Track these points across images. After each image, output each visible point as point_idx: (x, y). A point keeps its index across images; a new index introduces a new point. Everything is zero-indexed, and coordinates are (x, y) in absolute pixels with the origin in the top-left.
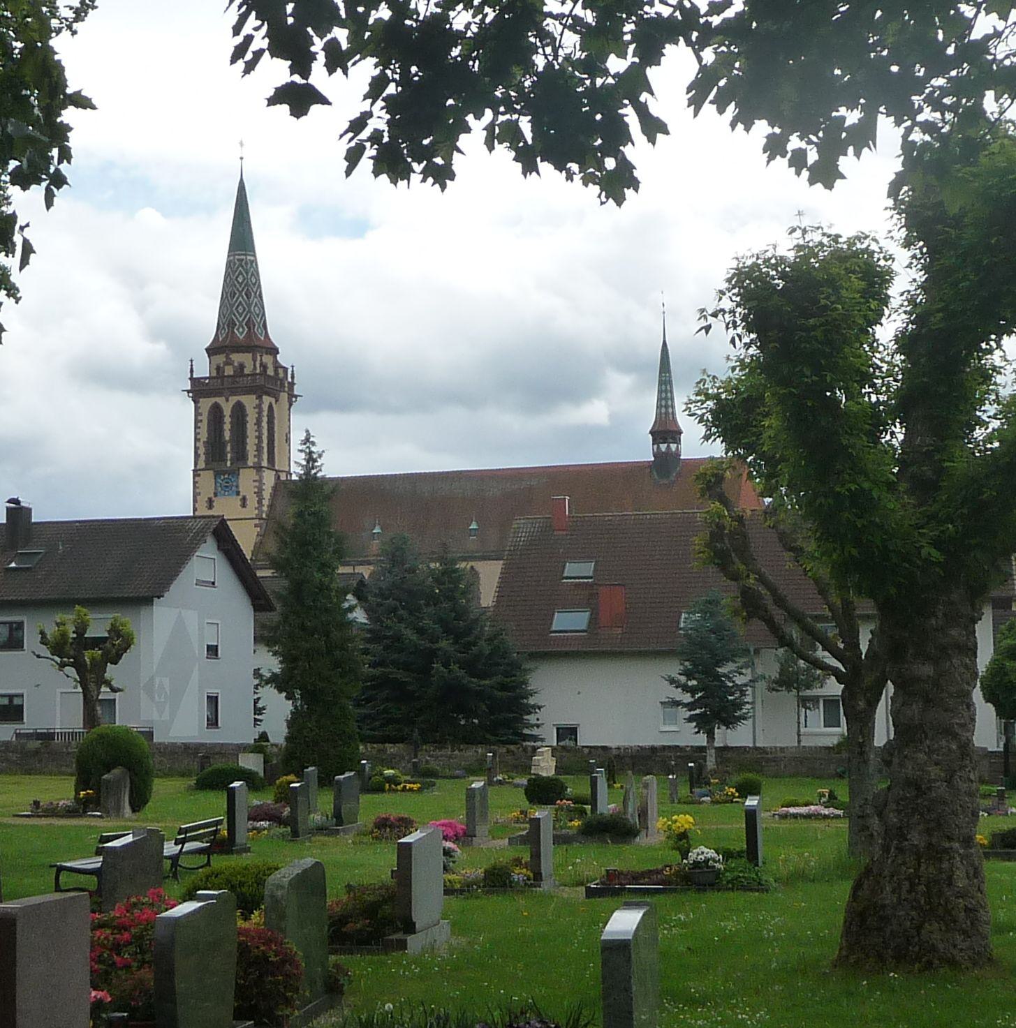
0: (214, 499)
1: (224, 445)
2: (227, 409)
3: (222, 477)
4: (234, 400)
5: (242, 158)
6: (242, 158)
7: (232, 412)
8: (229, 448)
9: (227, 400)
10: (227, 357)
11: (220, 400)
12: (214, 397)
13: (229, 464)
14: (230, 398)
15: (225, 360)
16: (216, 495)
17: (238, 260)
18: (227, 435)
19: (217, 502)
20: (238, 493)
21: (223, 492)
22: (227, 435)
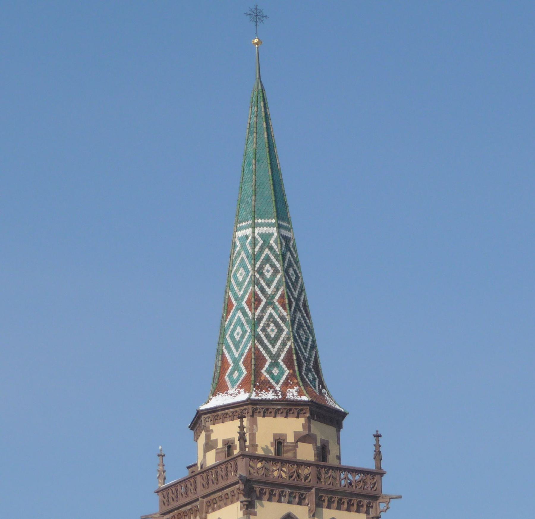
15: (300, 429)
17: (262, 235)
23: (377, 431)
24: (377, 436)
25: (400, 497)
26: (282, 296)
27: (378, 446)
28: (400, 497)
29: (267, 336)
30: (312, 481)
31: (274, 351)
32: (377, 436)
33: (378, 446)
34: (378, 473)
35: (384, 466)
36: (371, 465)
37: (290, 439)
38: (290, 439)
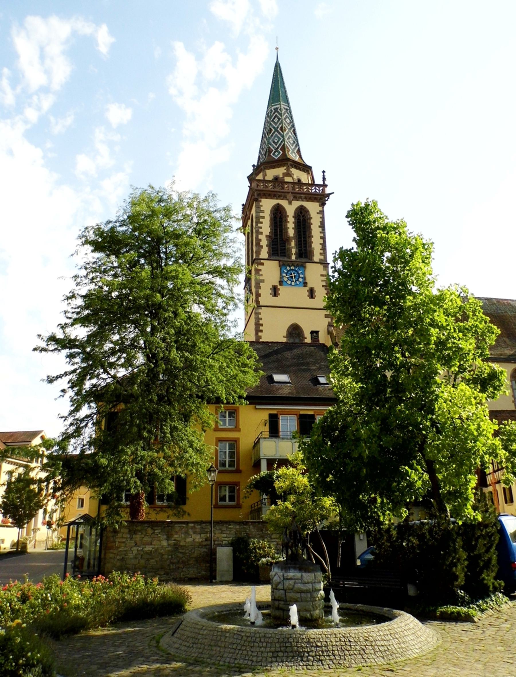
0: (279, 287)
1: (288, 240)
2: (290, 209)
3: (288, 268)
4: (296, 204)
5: (277, 49)
6: (277, 49)
7: (295, 213)
8: (293, 244)
9: (290, 203)
10: (288, 169)
11: (284, 203)
12: (277, 199)
13: (293, 257)
14: (293, 202)
15: (285, 171)
16: (281, 283)
18: (291, 232)
19: (282, 290)
20: (305, 284)
21: (289, 282)
22: (291, 232)
24: (324, 172)
27: (324, 176)
30: (291, 189)
31: (276, 147)
32: (324, 172)
33: (324, 176)
34: (325, 186)
35: (326, 183)
36: (322, 183)
37: (281, 176)
38: (281, 176)
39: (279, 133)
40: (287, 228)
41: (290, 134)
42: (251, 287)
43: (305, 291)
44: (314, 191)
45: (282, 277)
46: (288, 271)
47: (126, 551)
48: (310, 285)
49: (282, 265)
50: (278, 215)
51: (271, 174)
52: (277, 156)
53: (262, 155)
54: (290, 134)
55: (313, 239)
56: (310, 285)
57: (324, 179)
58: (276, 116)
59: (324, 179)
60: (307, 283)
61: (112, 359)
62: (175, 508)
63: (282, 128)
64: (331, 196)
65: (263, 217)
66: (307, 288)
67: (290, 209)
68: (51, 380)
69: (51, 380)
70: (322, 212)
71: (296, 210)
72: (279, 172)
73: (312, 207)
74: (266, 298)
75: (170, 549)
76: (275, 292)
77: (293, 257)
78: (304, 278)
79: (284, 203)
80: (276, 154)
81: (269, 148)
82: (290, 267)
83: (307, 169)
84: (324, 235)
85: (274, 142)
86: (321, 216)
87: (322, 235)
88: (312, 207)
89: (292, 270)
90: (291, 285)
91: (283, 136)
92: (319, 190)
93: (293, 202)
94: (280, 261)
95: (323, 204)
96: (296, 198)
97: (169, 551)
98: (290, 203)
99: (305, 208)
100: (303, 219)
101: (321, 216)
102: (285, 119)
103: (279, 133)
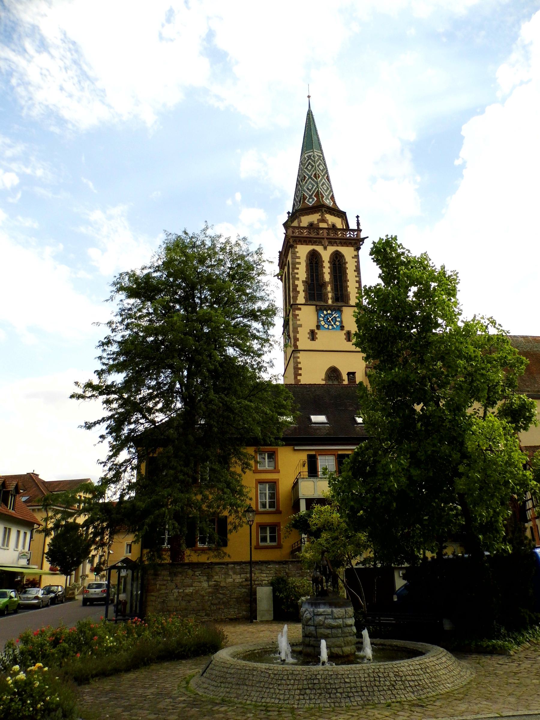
0: (316, 331)
1: (323, 285)
2: (326, 254)
3: (325, 312)
4: (331, 249)
5: (309, 97)
6: (309, 97)
7: (330, 258)
8: (329, 288)
9: (325, 248)
10: (322, 215)
11: (319, 249)
12: (312, 245)
13: (330, 302)
14: (328, 247)
15: (320, 217)
16: (318, 327)
18: (327, 277)
19: (320, 334)
20: (342, 328)
21: (326, 326)
22: (327, 277)
23: (459, 291)
24: (358, 217)
25: (368, 237)
26: (319, 177)
27: (358, 221)
28: (368, 237)
29: (308, 189)
30: (325, 235)
31: (310, 193)
32: (358, 217)
33: (358, 221)
34: (359, 230)
35: (361, 228)
36: (356, 228)
37: (316, 222)
38: (316, 222)
39: (313, 180)
40: (323, 274)
41: (323, 180)
42: (289, 332)
43: (342, 335)
44: (348, 236)
45: (319, 321)
46: (325, 315)
47: (166, 593)
48: (347, 329)
49: (319, 310)
50: (314, 260)
51: (305, 220)
52: (311, 203)
53: (297, 202)
54: (323, 180)
55: (349, 284)
56: (347, 329)
57: (358, 224)
58: (310, 163)
59: (358, 224)
60: (344, 327)
61: (150, 404)
62: (217, 550)
63: (315, 174)
64: (365, 240)
65: (299, 263)
66: (344, 332)
67: (326, 254)
68: (89, 426)
69: (89, 426)
70: (357, 257)
71: (332, 254)
72: (314, 218)
73: (347, 252)
74: (304, 342)
75: (210, 590)
76: (313, 335)
77: (330, 302)
78: (341, 322)
79: (319, 249)
80: (311, 200)
81: (304, 195)
82: (327, 311)
83: (342, 215)
84: (360, 279)
85: (308, 189)
86: (356, 260)
87: (357, 279)
88: (347, 252)
89: (329, 314)
90: (328, 329)
91: (317, 183)
92: (354, 235)
93: (328, 247)
94: (316, 306)
95: (358, 249)
96: (331, 244)
97: (209, 592)
98: (325, 248)
99: (340, 253)
100: (338, 261)
101: (356, 260)
102: (318, 166)
103: (313, 180)
